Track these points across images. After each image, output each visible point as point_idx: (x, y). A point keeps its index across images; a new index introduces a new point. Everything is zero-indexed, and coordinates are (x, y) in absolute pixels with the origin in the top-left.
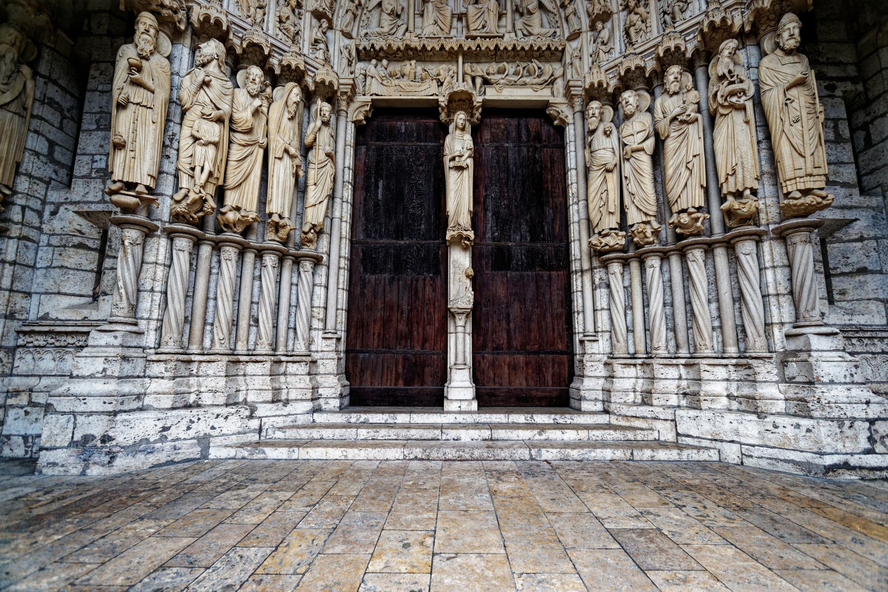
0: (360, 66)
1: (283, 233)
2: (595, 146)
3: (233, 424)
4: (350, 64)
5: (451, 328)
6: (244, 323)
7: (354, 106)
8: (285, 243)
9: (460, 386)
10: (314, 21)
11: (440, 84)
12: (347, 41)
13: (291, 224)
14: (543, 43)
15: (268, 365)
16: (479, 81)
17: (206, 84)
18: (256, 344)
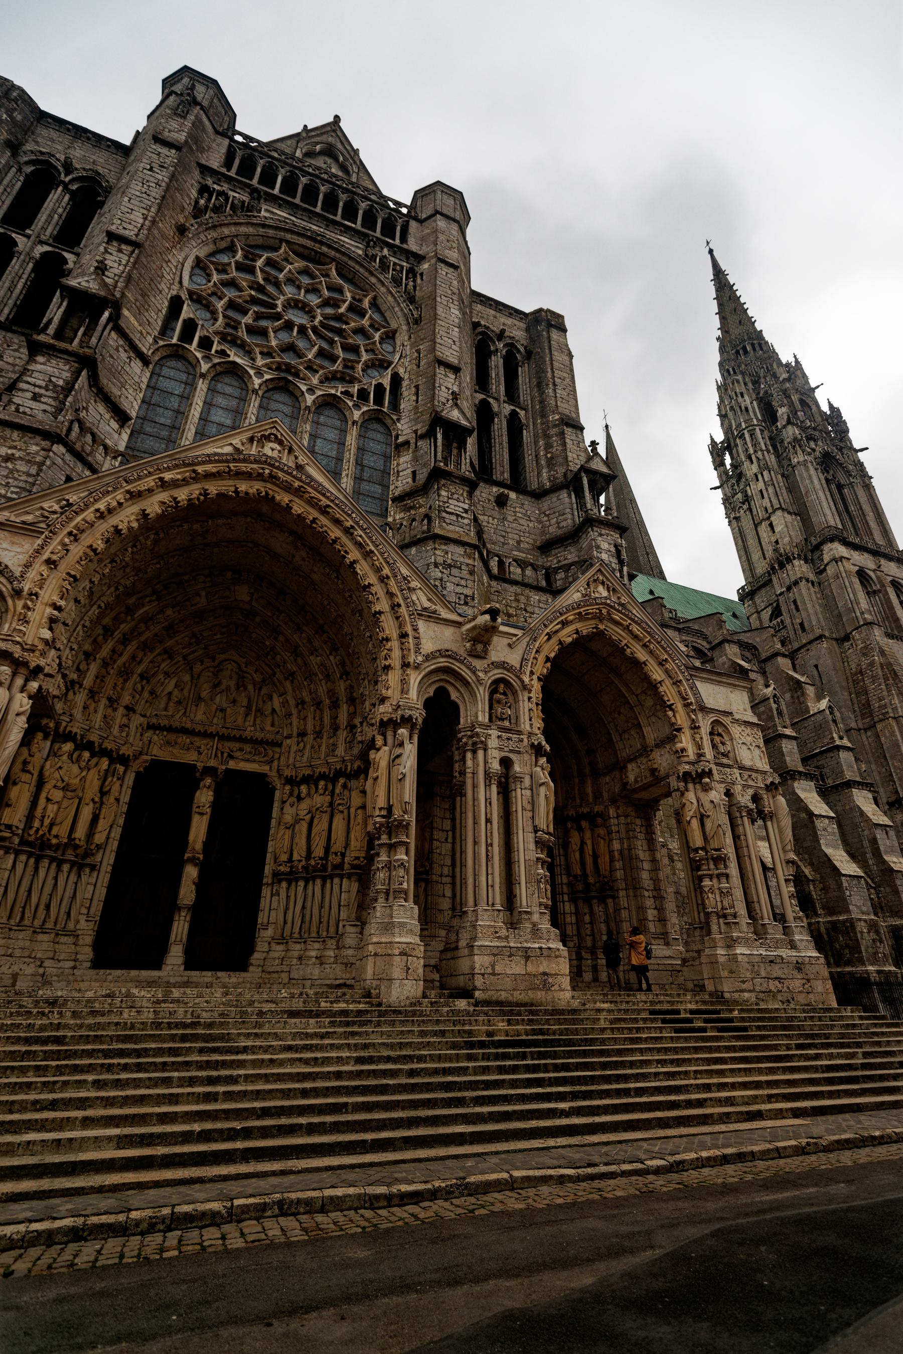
0: (148, 734)
1: (78, 851)
2: (285, 810)
3: (29, 970)
4: (142, 735)
5: (176, 918)
6: (42, 907)
7: (138, 761)
8: (76, 857)
9: (176, 955)
10: (125, 712)
11: (200, 753)
12: (142, 719)
13: (82, 843)
14: (270, 737)
15: (53, 935)
16: (225, 755)
17: (60, 768)
18: (44, 922)
